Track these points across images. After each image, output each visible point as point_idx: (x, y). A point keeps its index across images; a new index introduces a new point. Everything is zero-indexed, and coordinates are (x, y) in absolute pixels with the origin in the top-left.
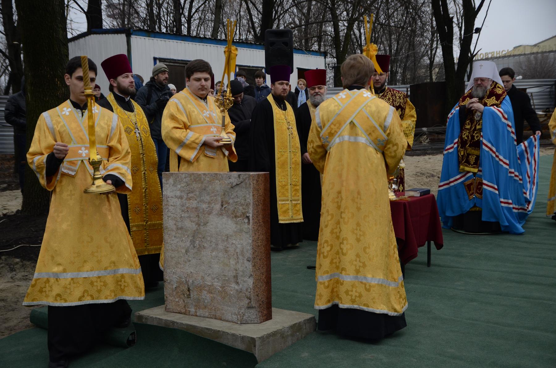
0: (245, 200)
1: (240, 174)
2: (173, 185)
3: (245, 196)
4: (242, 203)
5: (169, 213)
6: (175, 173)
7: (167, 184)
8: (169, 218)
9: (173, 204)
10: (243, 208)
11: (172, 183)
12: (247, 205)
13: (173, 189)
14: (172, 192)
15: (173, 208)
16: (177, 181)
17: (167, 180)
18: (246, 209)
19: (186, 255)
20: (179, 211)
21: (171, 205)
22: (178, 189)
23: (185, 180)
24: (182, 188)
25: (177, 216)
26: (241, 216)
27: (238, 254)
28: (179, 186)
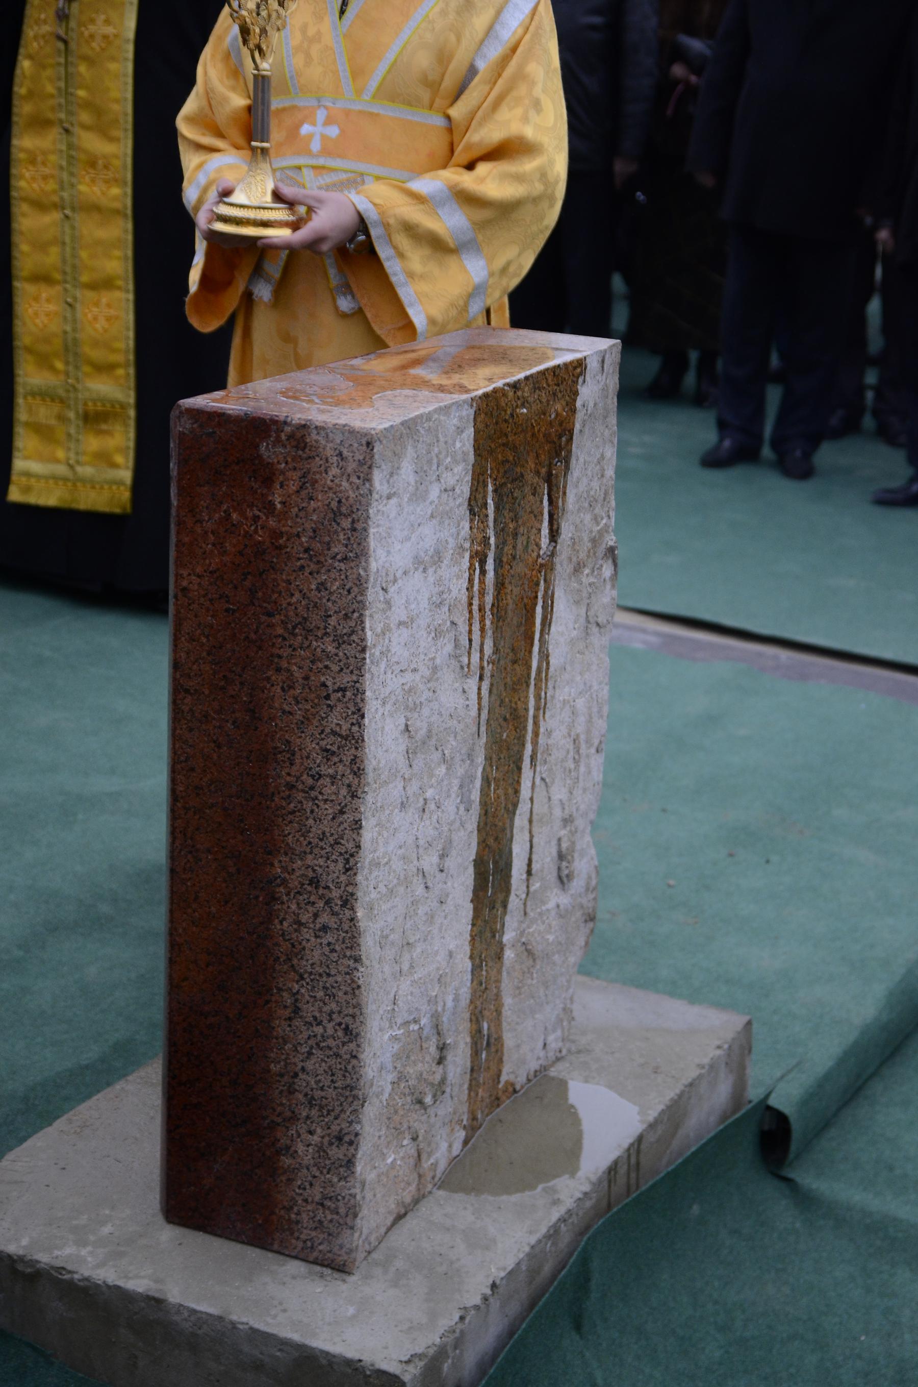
0: (602, 476)
1: (605, 351)
2: (410, 500)
3: (602, 455)
4: (592, 493)
5: (389, 675)
6: (421, 416)
7: (389, 497)
8: (388, 707)
9: (404, 618)
10: (596, 519)
11: (412, 479)
12: (605, 499)
13: (412, 518)
14: (408, 539)
15: (405, 633)
16: (430, 462)
17: (391, 474)
18: (602, 519)
19: (438, 875)
20: (424, 640)
21: (401, 623)
22: (429, 512)
23: (458, 445)
24: (445, 496)
25: (417, 677)
26: (588, 556)
27: (582, 737)
28: (434, 492)
